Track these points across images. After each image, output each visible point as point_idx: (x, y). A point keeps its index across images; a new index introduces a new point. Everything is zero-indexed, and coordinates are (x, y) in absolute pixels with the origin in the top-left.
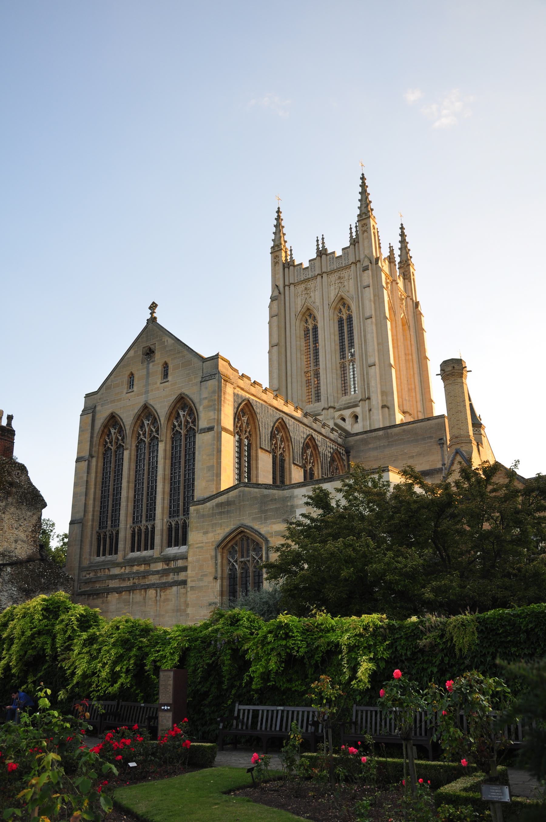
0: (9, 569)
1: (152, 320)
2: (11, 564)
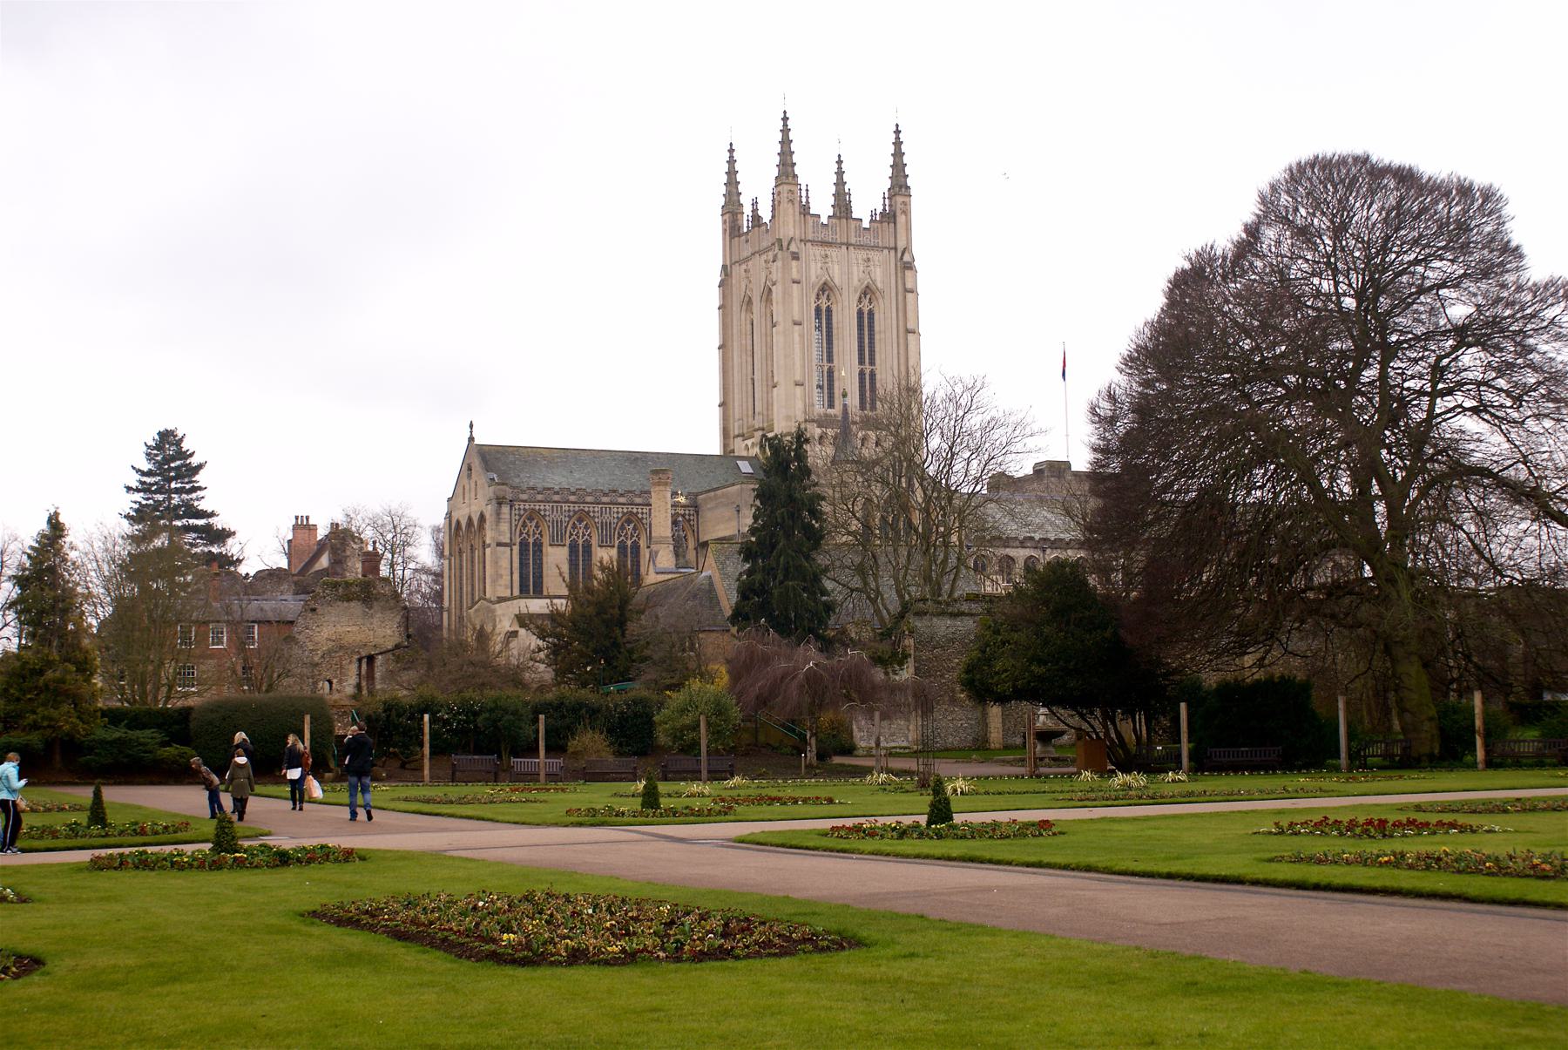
0: (380, 657)
1: (471, 439)
2: (381, 653)
